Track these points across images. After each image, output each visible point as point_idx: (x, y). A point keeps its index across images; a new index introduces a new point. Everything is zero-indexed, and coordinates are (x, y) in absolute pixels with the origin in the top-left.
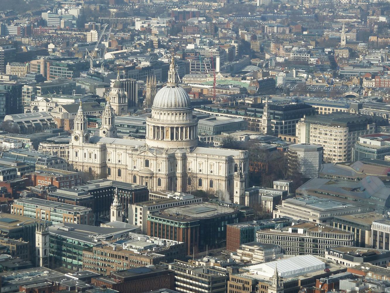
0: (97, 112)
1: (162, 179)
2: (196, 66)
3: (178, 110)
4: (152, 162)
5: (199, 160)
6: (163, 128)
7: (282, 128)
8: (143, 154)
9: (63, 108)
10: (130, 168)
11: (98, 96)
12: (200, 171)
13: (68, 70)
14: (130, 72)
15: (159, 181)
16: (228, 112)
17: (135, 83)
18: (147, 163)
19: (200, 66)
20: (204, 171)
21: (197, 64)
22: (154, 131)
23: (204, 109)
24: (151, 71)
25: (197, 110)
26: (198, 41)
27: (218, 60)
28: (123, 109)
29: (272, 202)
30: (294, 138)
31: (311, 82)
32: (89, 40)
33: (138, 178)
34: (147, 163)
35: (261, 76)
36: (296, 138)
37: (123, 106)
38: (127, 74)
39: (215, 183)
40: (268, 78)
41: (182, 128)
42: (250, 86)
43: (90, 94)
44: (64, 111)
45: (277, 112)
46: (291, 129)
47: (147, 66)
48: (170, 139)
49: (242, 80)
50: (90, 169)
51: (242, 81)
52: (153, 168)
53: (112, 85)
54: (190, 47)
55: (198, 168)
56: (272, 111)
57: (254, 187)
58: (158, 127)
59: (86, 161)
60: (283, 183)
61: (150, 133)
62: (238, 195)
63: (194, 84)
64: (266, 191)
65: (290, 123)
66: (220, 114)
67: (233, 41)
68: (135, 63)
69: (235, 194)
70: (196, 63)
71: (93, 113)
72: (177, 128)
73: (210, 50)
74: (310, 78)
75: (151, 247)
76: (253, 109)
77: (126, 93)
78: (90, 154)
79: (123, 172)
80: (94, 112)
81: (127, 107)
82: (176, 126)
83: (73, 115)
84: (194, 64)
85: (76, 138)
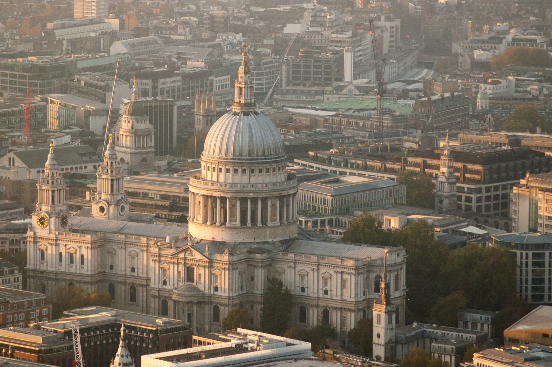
0: (90, 167)
1: (222, 308)
2: (302, 70)
3: (257, 163)
5: (323, 270)
6: (223, 200)
7: (479, 200)
8: (182, 255)
9: (16, 159)
10: (155, 284)
11: (93, 134)
12: (326, 292)
13: (31, 78)
14: (164, 84)
15: (216, 310)
16: (366, 168)
17: (172, 107)
19: (312, 70)
20: (334, 293)
21: (305, 66)
22: (206, 206)
23: (315, 159)
24: (207, 79)
25: (301, 162)
26: (307, 15)
27: (348, 58)
28: (144, 160)
29: (453, 358)
30: (505, 221)
31: (546, 103)
33: (171, 305)
35: (440, 89)
36: (509, 222)
37: (146, 153)
38: (155, 87)
40: (452, 94)
41: (264, 200)
42: (415, 110)
43: (76, 129)
44: (18, 163)
45: (470, 166)
46: (500, 201)
47: (198, 70)
48: (238, 223)
49: (400, 99)
50: (71, 284)
51: (400, 102)
53: (123, 109)
54: (292, 29)
55: (321, 286)
56: (459, 165)
57: (415, 325)
58: (214, 198)
59: (62, 269)
60: (478, 316)
61: (196, 210)
62: (382, 341)
63: (297, 108)
64: (440, 332)
65: (496, 188)
66: (348, 171)
67: (383, 18)
68: (174, 63)
69: (375, 339)
70: (302, 64)
71: (81, 168)
72: (254, 200)
73: (334, 36)
74: (545, 95)
76: (419, 160)
77: (151, 127)
79: (141, 293)
80: (83, 166)
81: (153, 155)
82: (251, 195)
83: (39, 172)
84: (298, 66)
85: (42, 221)
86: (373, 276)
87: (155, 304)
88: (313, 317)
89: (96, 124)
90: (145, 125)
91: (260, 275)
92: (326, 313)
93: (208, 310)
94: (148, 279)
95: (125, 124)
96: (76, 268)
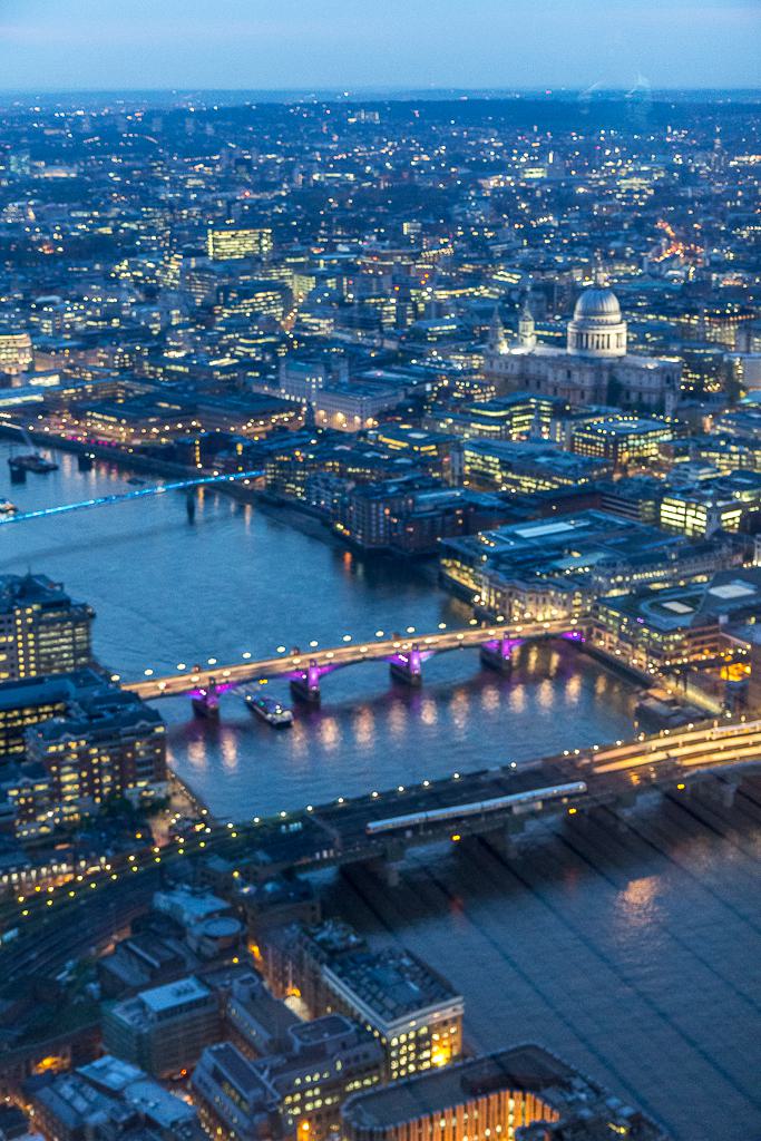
4: (576, 374)
10: (551, 379)
18: (569, 374)
32: (500, 235)
34: (569, 374)
39: (645, 398)
50: (506, 380)
52: (576, 377)
53: (529, 289)
54: (614, 244)
75: (575, 466)
78: (507, 363)
79: (543, 385)
86: (665, 375)
87: (550, 390)
88: (634, 397)
89: (515, 296)
90: (540, 296)
91: (606, 374)
92: (640, 394)
93: (578, 393)
94: (546, 377)
95: (531, 295)
96: (509, 370)
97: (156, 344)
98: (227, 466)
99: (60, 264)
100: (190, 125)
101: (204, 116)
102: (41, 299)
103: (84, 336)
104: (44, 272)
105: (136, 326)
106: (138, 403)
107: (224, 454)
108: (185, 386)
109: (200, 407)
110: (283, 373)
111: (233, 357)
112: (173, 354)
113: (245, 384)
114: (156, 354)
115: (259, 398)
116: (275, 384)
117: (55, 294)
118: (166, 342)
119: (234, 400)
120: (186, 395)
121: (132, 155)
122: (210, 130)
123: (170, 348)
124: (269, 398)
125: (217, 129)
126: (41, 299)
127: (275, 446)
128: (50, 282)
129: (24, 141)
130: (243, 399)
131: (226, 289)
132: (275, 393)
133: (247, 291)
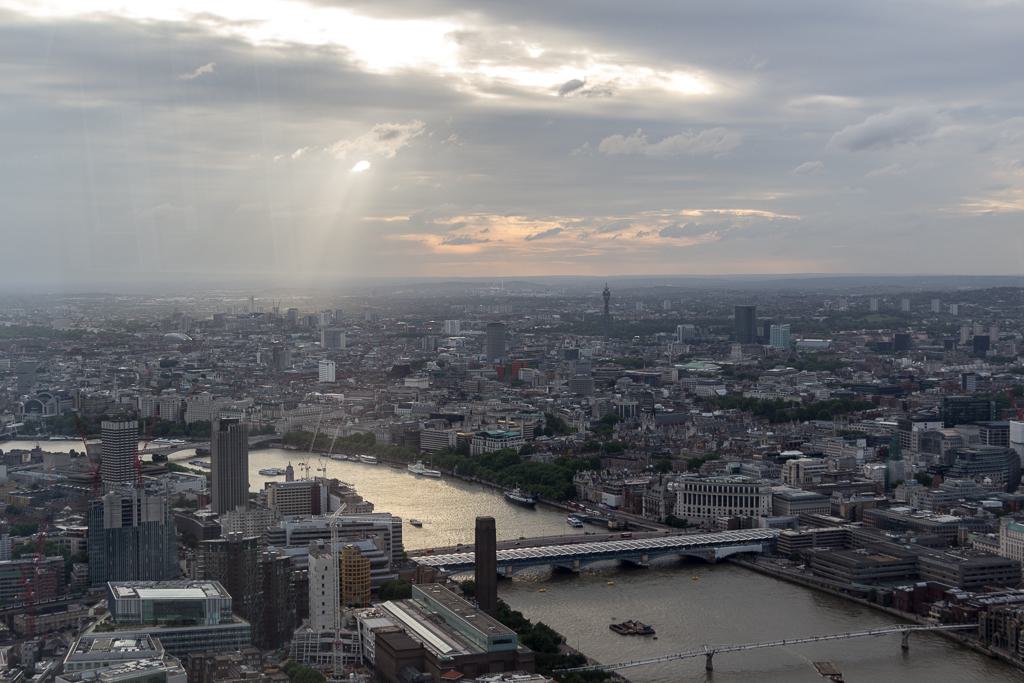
97: (885, 498)
98: (943, 616)
99: (807, 423)
100: (936, 306)
101: (947, 298)
102: (786, 453)
103: (819, 488)
104: (790, 430)
105: (868, 481)
106: (863, 551)
107: (940, 604)
108: (908, 540)
109: (920, 558)
110: (1002, 529)
111: (955, 514)
112: (900, 509)
113: (966, 539)
114: (886, 504)
115: (976, 554)
116: (996, 540)
117: (798, 450)
118: (894, 497)
119: (953, 553)
120: (908, 547)
121: (880, 331)
122: (954, 309)
123: (898, 504)
124: (990, 555)
125: (959, 308)
126: (786, 453)
127: (990, 601)
128: (796, 438)
129: (788, 317)
130: (962, 555)
131: (951, 454)
132: (993, 550)
133: (974, 455)
